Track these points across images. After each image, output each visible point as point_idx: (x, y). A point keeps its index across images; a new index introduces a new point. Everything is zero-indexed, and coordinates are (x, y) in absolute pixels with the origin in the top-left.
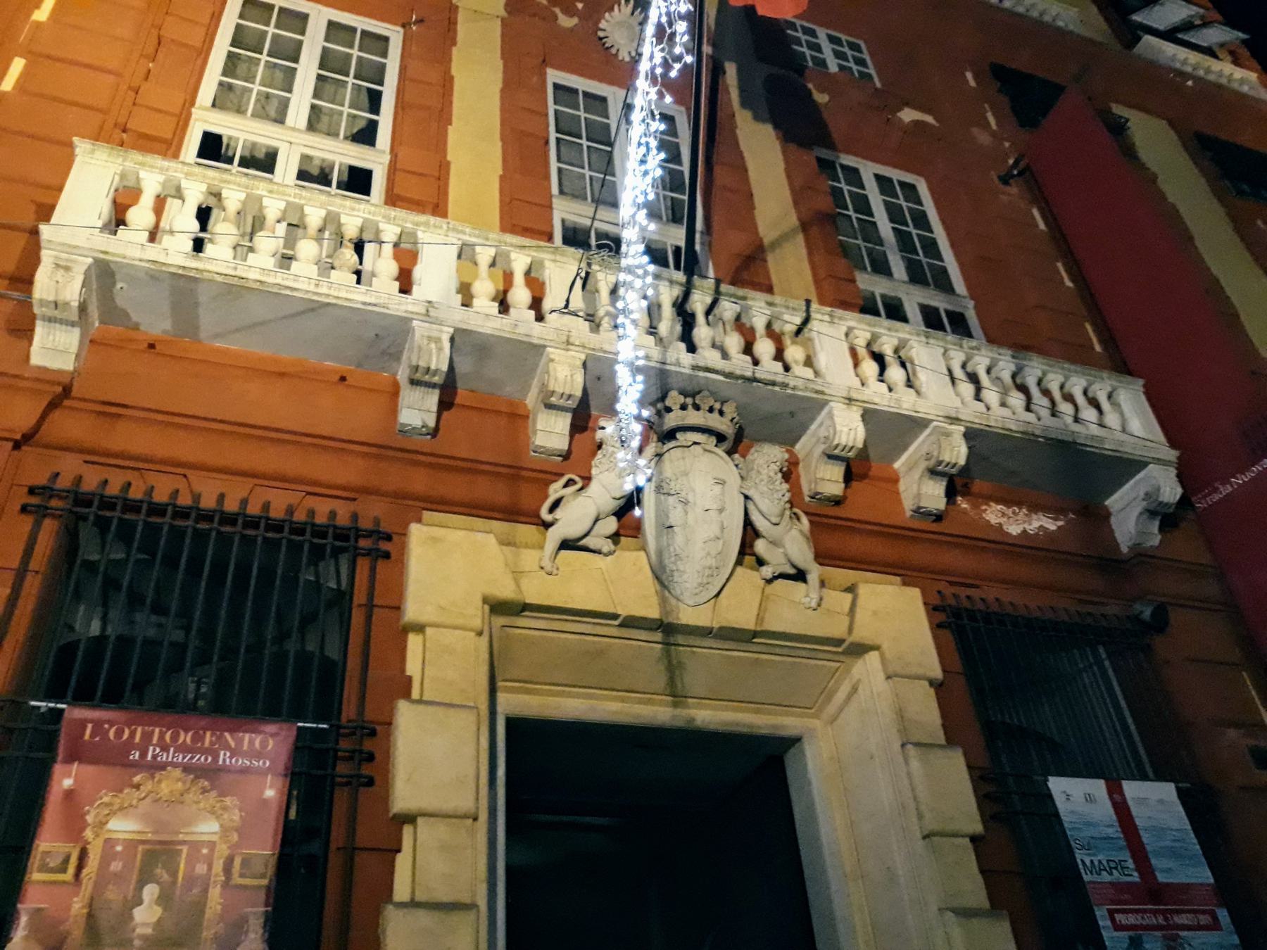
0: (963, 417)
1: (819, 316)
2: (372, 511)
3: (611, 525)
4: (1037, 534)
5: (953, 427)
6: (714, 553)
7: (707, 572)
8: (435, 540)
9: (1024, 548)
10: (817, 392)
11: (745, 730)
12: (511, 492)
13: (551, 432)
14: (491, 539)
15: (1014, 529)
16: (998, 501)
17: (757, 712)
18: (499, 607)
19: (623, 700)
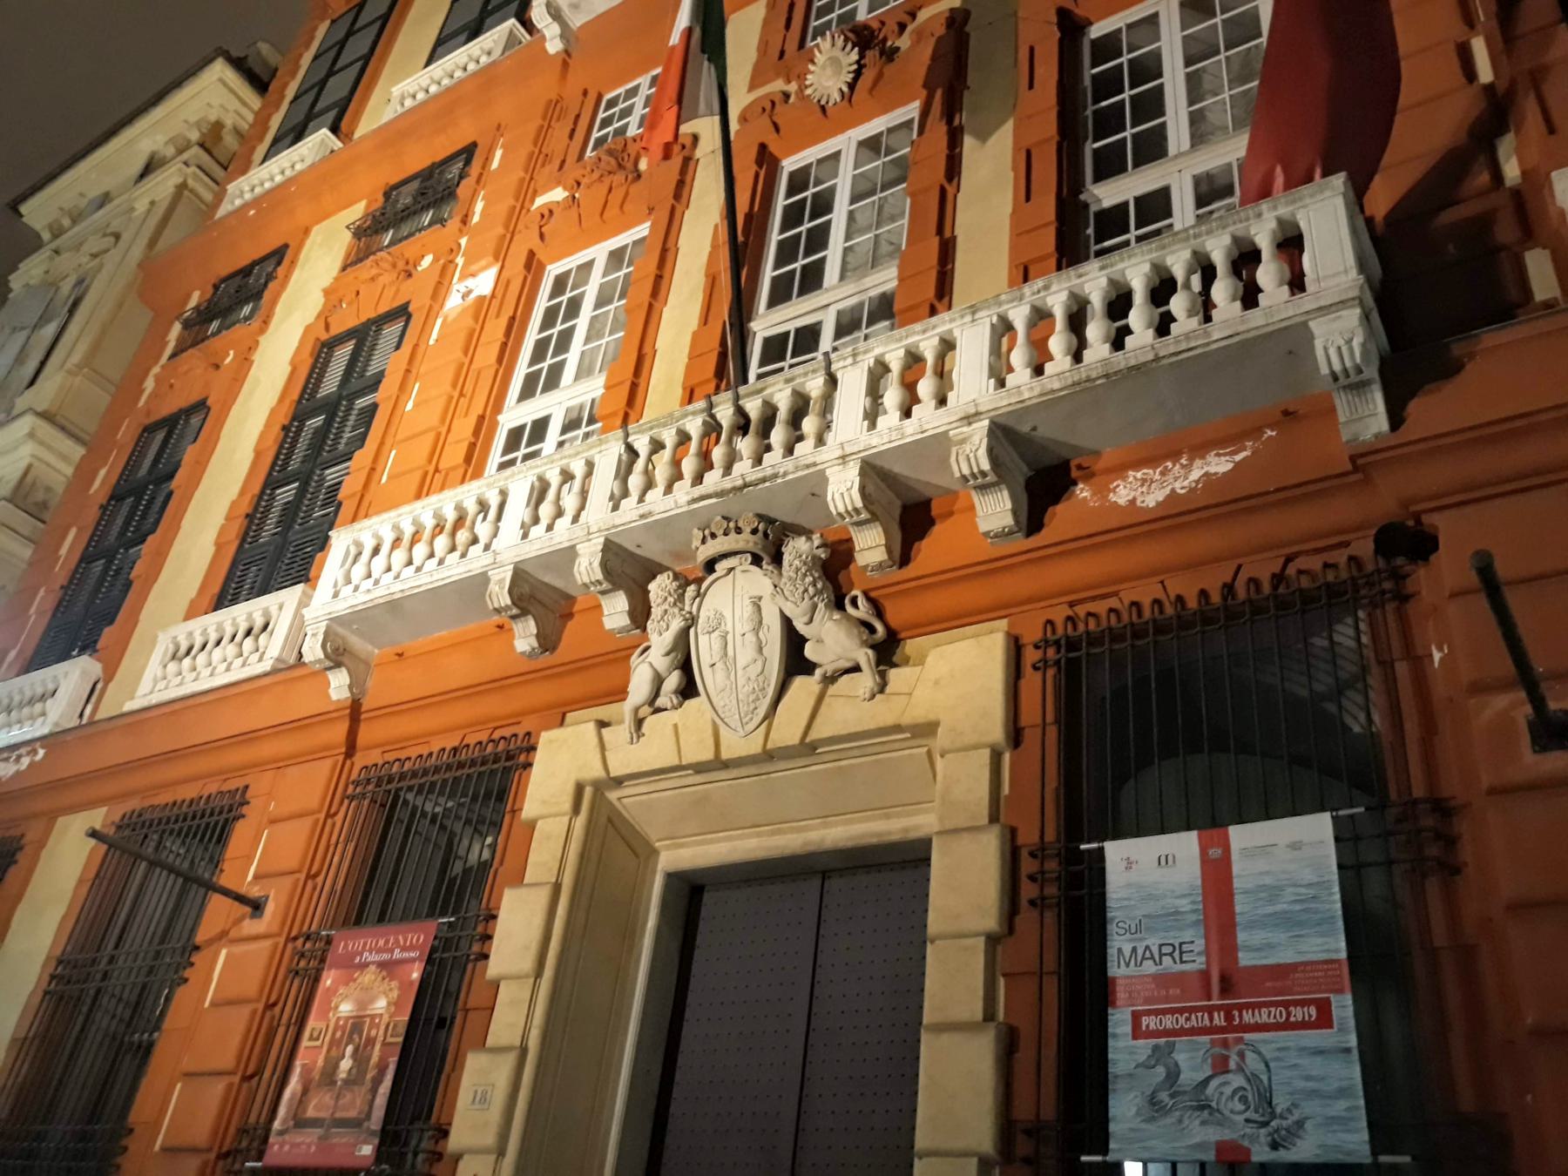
0: (982, 409)
1: (841, 364)
2: (521, 730)
3: (673, 681)
4: (1192, 490)
5: (974, 426)
6: (753, 677)
7: (752, 697)
8: (551, 741)
9: (1176, 517)
10: (808, 466)
11: (874, 840)
12: (595, 681)
13: (615, 611)
14: (591, 726)
15: (1152, 498)
16: (1137, 464)
17: (888, 817)
18: (600, 787)
19: (759, 835)
